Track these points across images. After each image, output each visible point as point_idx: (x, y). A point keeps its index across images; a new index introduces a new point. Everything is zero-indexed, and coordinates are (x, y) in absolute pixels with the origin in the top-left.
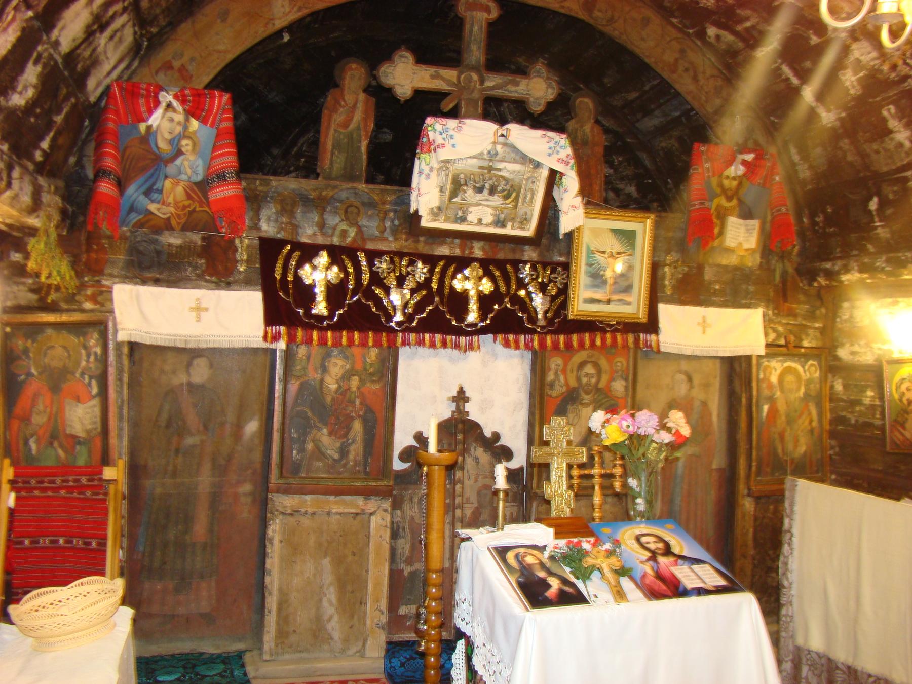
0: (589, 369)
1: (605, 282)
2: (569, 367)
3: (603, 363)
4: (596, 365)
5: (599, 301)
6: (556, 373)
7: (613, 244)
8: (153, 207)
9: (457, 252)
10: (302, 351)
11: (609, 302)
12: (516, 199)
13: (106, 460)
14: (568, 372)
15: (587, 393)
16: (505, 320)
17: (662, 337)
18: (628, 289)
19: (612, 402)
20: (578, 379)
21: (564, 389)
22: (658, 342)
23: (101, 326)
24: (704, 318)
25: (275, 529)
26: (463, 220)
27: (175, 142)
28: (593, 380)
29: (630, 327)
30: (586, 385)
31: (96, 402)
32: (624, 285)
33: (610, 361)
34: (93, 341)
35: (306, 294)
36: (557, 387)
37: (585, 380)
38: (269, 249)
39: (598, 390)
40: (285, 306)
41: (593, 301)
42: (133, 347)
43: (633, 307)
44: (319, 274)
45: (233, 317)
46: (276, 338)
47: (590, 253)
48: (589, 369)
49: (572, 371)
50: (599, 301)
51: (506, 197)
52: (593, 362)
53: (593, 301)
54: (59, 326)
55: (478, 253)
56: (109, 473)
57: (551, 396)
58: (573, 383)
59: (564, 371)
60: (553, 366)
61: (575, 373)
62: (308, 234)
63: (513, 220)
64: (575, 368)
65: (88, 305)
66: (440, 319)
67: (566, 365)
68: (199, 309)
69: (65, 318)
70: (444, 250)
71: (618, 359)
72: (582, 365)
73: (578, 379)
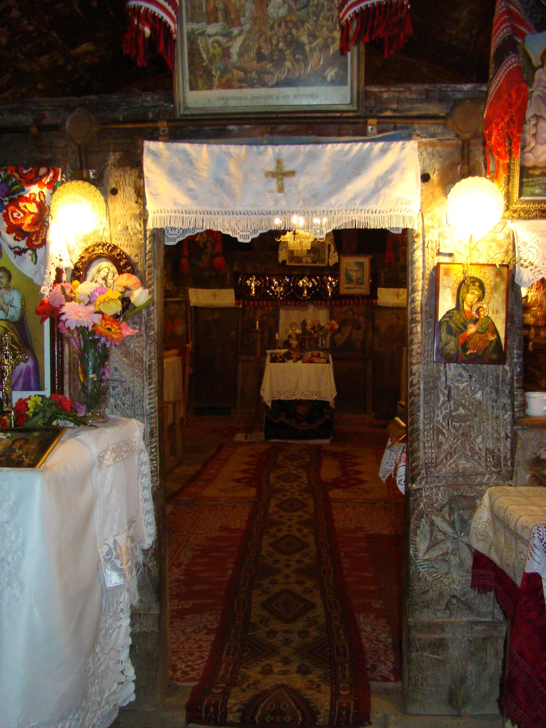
1: (353, 281)
4: (352, 311)
5: (351, 288)
7: (355, 268)
8: (200, 264)
9: (300, 273)
10: (248, 308)
11: (355, 288)
12: (319, 254)
13: (188, 342)
16: (318, 296)
17: (378, 301)
18: (362, 283)
22: (376, 302)
23: (187, 301)
24: (398, 293)
25: (240, 366)
26: (301, 262)
27: (205, 244)
29: (364, 297)
31: (184, 325)
32: (360, 282)
34: (183, 306)
35: (249, 289)
38: (236, 275)
40: (242, 293)
41: (348, 288)
42: (195, 307)
43: (364, 290)
44: (252, 284)
45: (226, 298)
46: (239, 304)
47: (347, 271)
48: (350, 313)
50: (351, 288)
51: (315, 253)
53: (348, 288)
54: (172, 302)
55: (307, 273)
56: (187, 346)
62: (249, 269)
63: (319, 261)
65: (181, 295)
66: (294, 297)
68: (215, 295)
69: (174, 299)
70: (296, 273)
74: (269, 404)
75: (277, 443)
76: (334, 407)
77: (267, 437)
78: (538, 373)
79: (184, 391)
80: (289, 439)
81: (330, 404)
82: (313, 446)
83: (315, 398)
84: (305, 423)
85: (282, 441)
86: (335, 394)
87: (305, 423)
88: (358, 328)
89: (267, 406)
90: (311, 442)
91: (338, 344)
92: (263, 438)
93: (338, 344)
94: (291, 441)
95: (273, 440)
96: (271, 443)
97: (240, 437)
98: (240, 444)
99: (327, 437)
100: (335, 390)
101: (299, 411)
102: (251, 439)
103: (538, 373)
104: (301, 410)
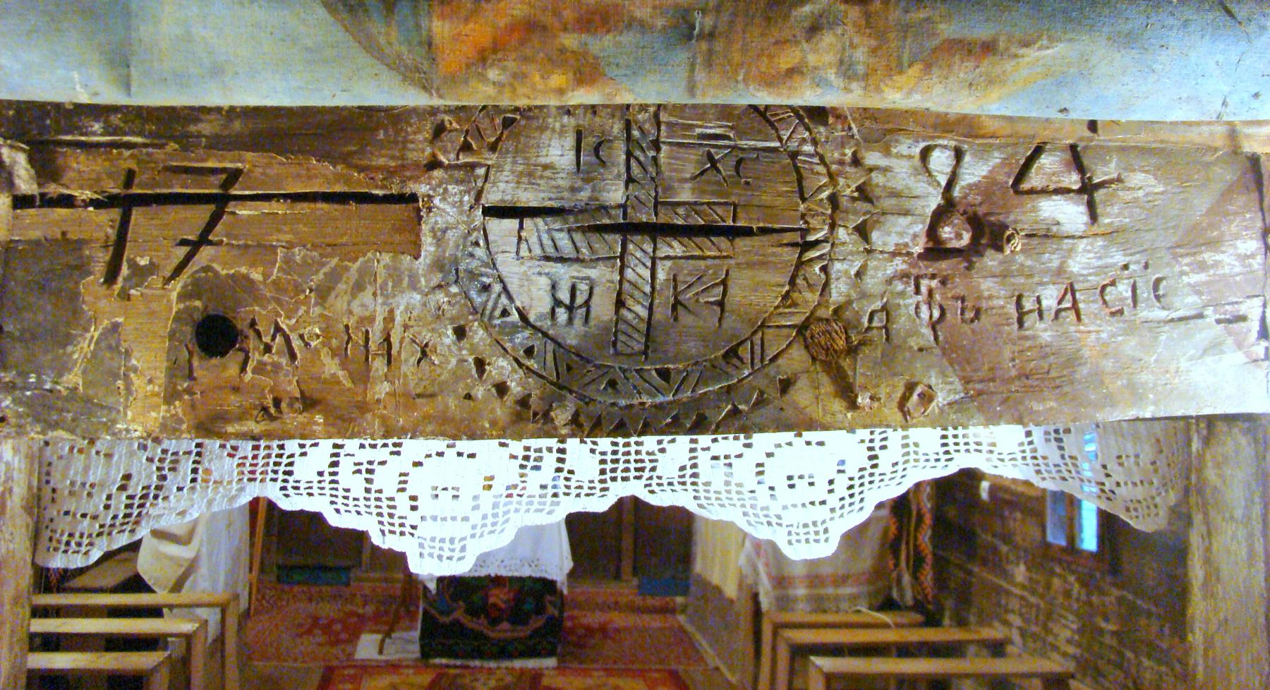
74: (432, 586)
75: (447, 666)
76: (565, 592)
77: (426, 654)
78: (1004, 549)
79: (251, 570)
80: (474, 658)
81: (559, 585)
82: (523, 672)
83: (526, 572)
84: (505, 625)
85: (459, 662)
86: (568, 564)
87: (505, 625)
89: (425, 588)
90: (518, 664)
92: (414, 650)
94: (477, 663)
95: (437, 661)
96: (435, 666)
97: (367, 647)
98: (367, 669)
99: (550, 654)
100: (570, 557)
101: (492, 600)
102: (393, 653)
103: (1004, 549)
104: (498, 597)
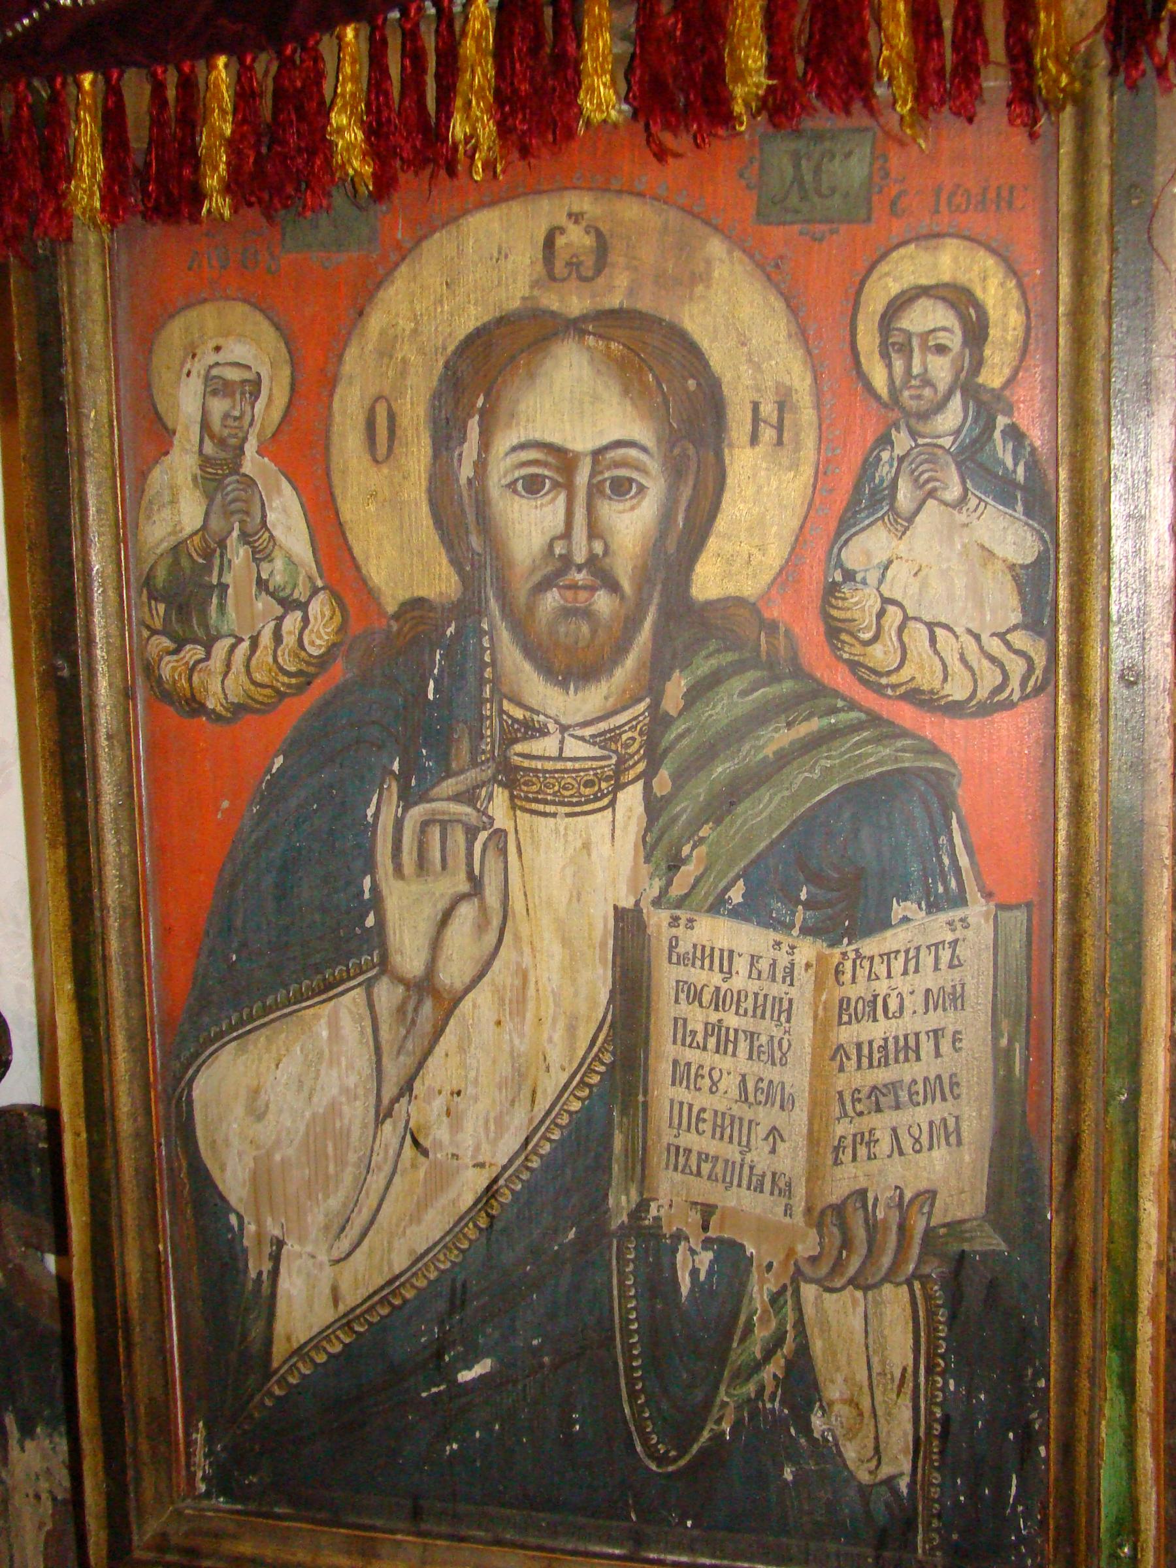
0: (574, 404)
2: (349, 406)
3: (740, 324)
6: (220, 471)
14: (348, 443)
15: (574, 669)
19: (878, 758)
20: (461, 518)
21: (320, 626)
28: (631, 525)
30: (556, 568)
33: (820, 312)
36: (241, 610)
37: (530, 525)
39: (688, 626)
48: (574, 404)
49: (381, 437)
52: (608, 321)
57: (194, 706)
58: (403, 561)
59: (303, 449)
60: (186, 403)
61: (417, 454)
64: (414, 411)
67: (313, 385)
71: (906, 268)
72: (486, 366)
73: (461, 518)
88: (835, 877)
91: (306, 1300)
93: (306, 1300)
